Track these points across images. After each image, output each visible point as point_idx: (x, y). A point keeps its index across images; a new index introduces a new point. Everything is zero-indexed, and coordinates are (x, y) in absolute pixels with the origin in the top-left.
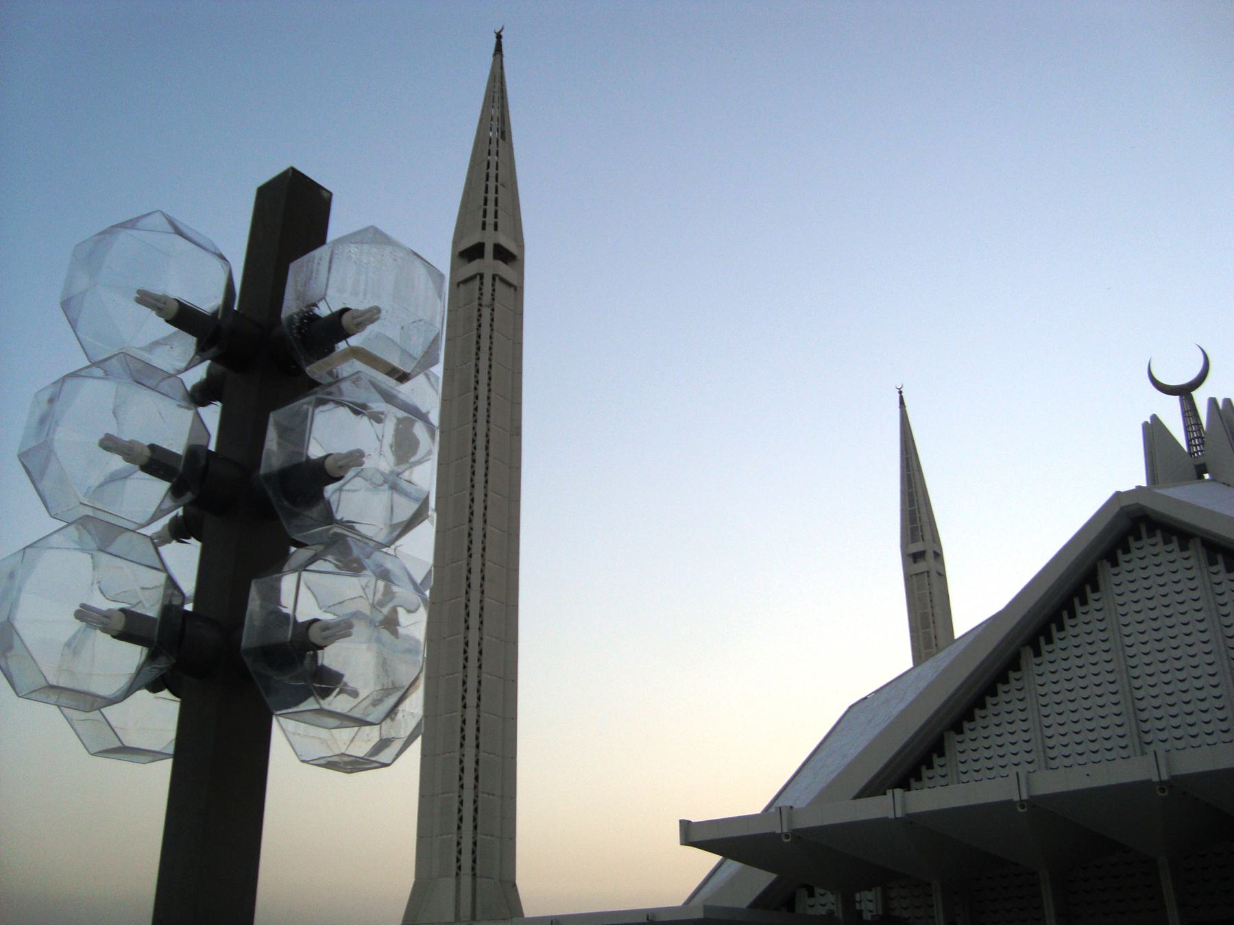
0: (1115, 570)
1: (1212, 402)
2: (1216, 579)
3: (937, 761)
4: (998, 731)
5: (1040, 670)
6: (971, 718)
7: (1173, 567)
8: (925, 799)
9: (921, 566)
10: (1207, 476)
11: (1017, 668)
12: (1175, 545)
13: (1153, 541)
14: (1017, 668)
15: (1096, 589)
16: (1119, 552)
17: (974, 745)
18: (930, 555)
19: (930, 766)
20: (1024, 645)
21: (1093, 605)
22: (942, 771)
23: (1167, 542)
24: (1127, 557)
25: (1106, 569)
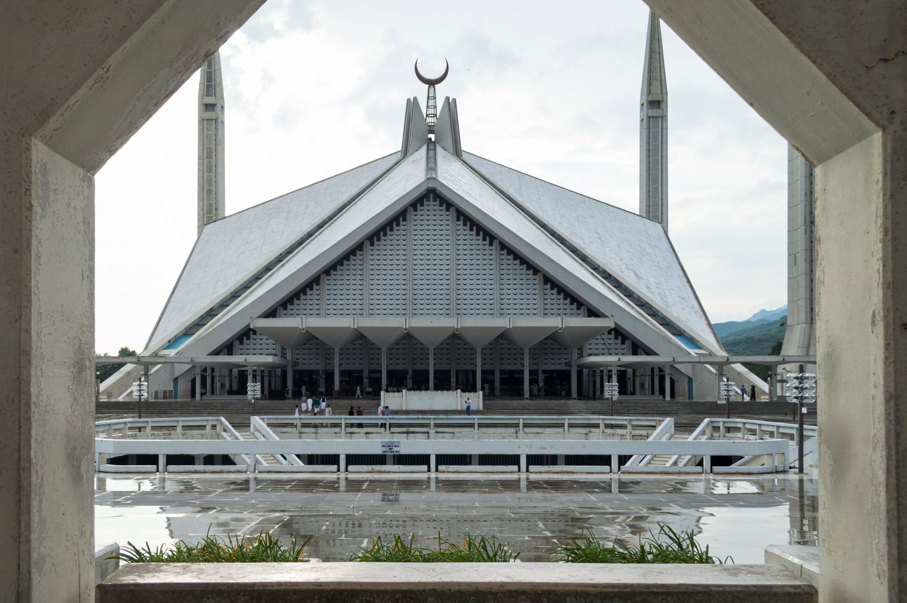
0: (415, 213)
1: (448, 98)
2: (459, 228)
3: (315, 287)
4: (348, 277)
5: (372, 253)
6: (335, 270)
7: (441, 218)
10: (432, 136)
12: (444, 208)
15: (404, 220)
17: (335, 282)
18: (219, 106)
19: (312, 289)
22: (318, 292)
23: (441, 205)
24: (422, 208)
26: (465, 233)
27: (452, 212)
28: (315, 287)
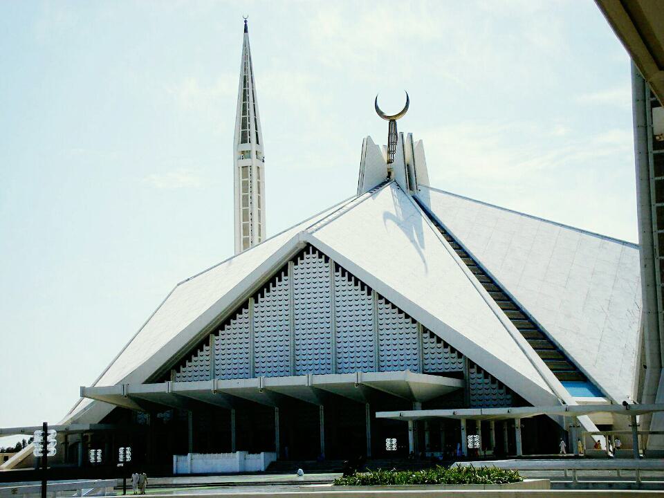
0: (296, 267)
2: (337, 279)
3: (205, 348)
8: (179, 386)
9: (246, 162)
11: (247, 307)
13: (314, 256)
14: (247, 307)
15: (286, 275)
16: (299, 259)
20: (251, 297)
21: (284, 282)
22: (208, 353)
23: (320, 257)
24: (302, 261)
25: (291, 266)
26: (344, 283)
27: (331, 265)
28: (205, 348)
